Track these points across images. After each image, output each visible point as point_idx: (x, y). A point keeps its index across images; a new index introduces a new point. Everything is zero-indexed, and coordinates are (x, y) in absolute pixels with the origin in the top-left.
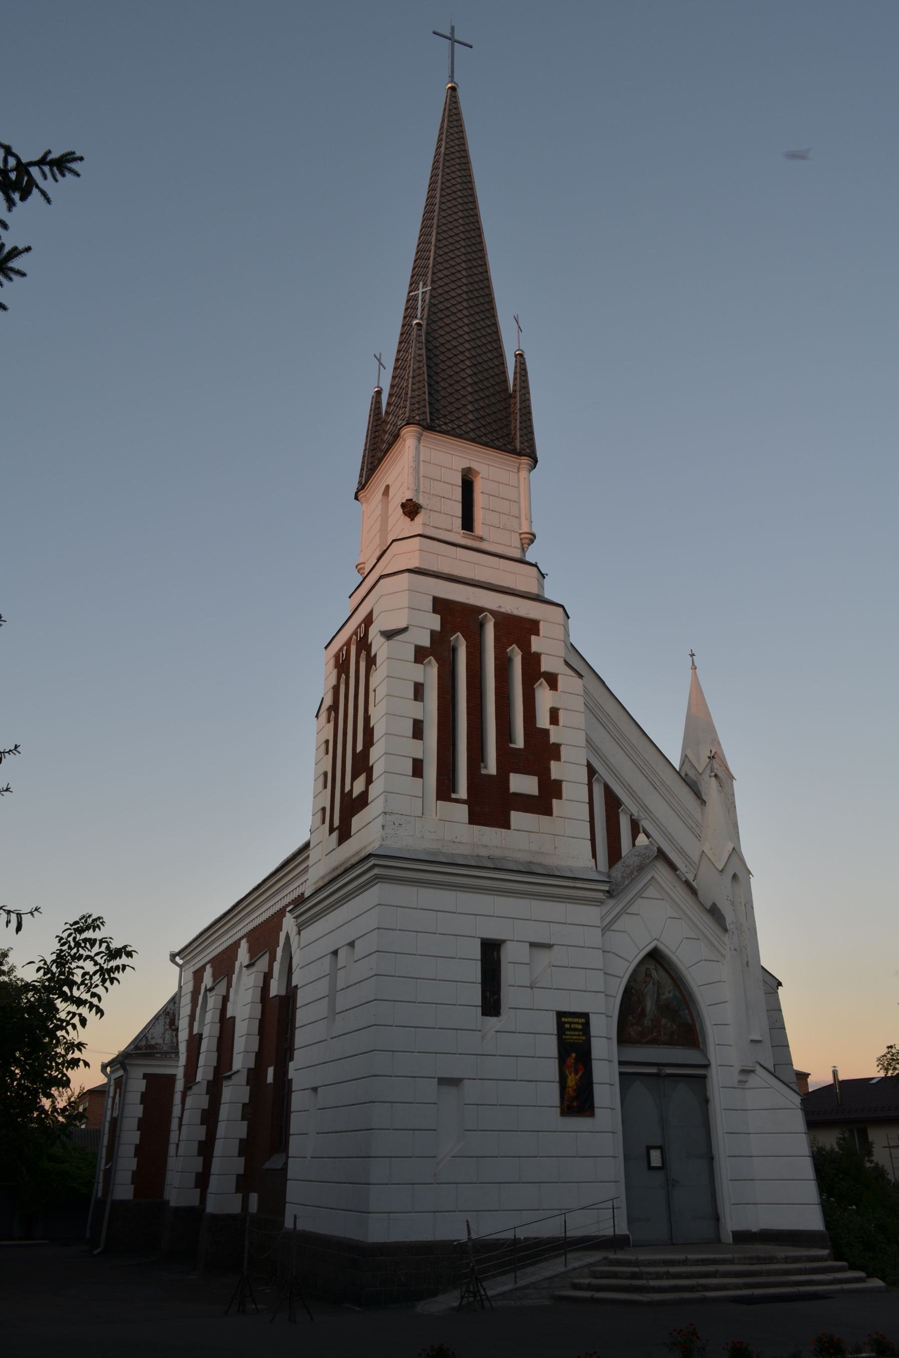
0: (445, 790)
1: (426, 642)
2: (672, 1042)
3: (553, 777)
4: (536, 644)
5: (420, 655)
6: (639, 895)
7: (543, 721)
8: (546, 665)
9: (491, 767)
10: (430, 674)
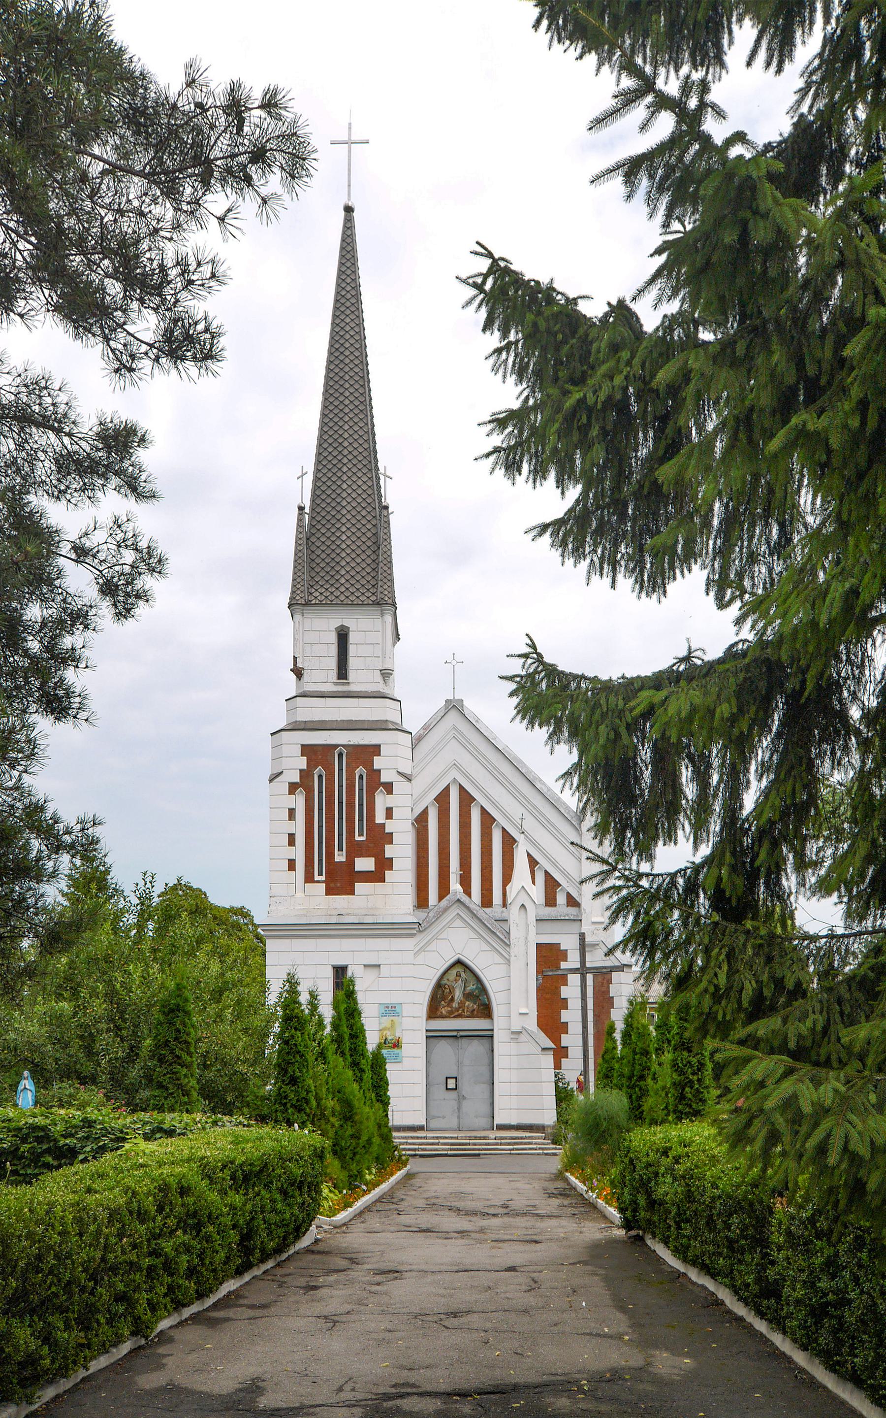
0: (309, 878)
1: (296, 779)
2: (472, 1015)
3: (387, 856)
4: (378, 763)
5: (293, 788)
6: (448, 926)
7: (380, 818)
8: (383, 779)
9: (340, 857)
10: (299, 801)
